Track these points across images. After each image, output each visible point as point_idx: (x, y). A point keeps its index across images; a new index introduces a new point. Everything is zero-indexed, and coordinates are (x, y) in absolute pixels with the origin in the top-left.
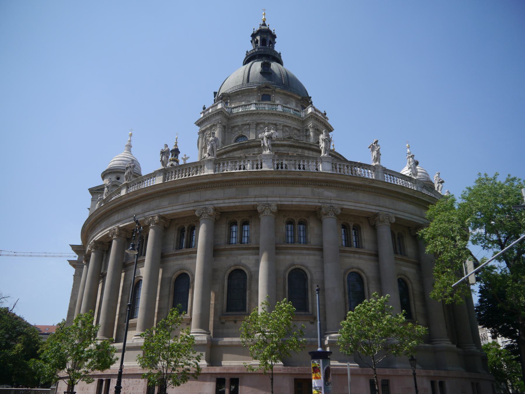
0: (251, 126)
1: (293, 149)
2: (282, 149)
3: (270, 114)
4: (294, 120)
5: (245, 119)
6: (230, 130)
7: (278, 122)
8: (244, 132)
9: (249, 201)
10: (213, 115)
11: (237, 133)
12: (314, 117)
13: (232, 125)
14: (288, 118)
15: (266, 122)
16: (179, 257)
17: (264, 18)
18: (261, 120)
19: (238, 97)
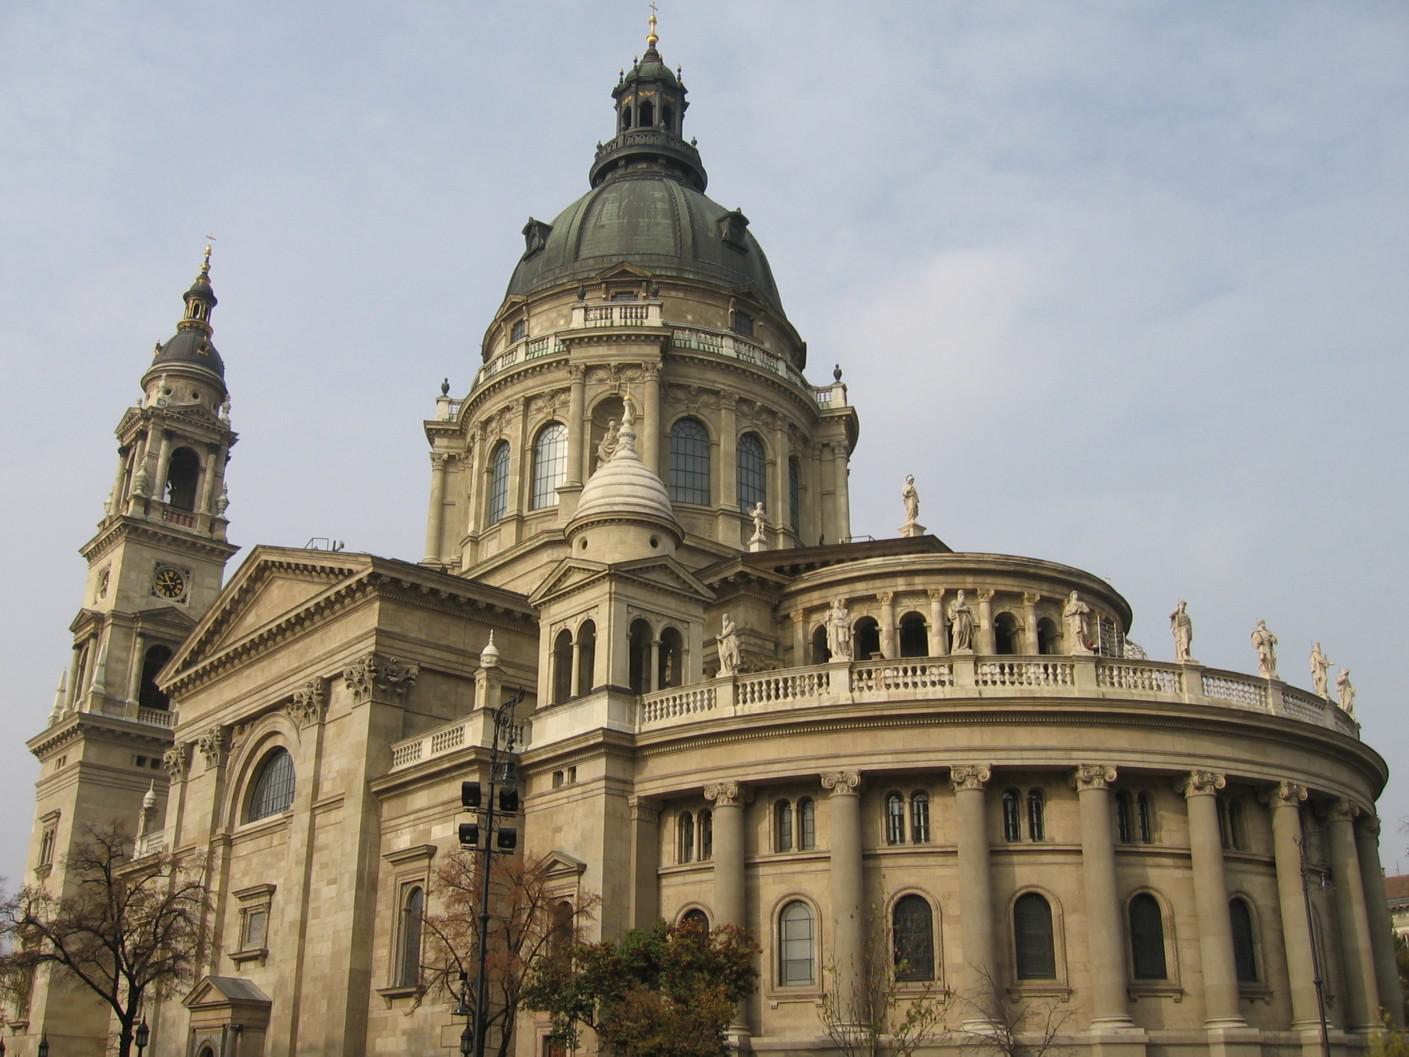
5: (710, 375)
10: (638, 336)
11: (684, 408)
13: (673, 380)
19: (673, 294)
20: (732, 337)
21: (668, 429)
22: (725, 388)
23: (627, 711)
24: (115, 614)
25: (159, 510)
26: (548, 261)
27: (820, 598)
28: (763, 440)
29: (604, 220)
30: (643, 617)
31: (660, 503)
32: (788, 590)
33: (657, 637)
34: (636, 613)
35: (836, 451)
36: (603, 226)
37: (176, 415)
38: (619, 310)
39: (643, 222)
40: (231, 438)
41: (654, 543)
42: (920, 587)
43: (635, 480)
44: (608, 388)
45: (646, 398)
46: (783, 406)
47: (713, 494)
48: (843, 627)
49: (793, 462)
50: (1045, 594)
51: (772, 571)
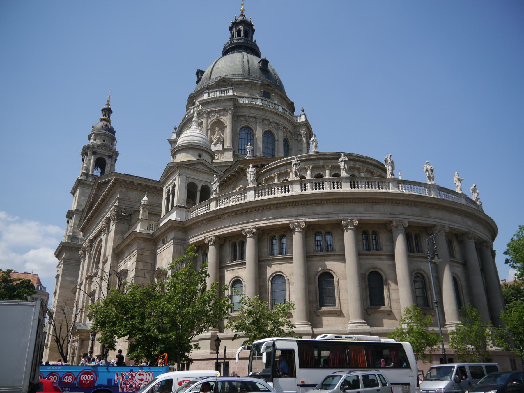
0: (258, 120)
1: (376, 169)
2: (370, 167)
5: (253, 111)
6: (236, 118)
8: (250, 124)
9: (431, 221)
10: (224, 99)
11: (243, 123)
12: (307, 125)
13: (239, 114)
14: (287, 121)
15: (271, 120)
16: (369, 257)
17: (242, 8)
19: (241, 86)
20: (261, 99)
21: (238, 130)
23: (184, 214)
24: (76, 210)
25: (91, 177)
26: (202, 82)
27: (270, 174)
29: (219, 66)
30: (193, 181)
32: (259, 173)
33: (199, 188)
34: (190, 180)
36: (219, 68)
37: (96, 147)
40: (117, 154)
41: (200, 156)
43: (193, 134)
44: (215, 118)
45: (228, 119)
46: (282, 121)
47: (254, 151)
48: (253, 174)
49: (286, 140)
50: (352, 165)
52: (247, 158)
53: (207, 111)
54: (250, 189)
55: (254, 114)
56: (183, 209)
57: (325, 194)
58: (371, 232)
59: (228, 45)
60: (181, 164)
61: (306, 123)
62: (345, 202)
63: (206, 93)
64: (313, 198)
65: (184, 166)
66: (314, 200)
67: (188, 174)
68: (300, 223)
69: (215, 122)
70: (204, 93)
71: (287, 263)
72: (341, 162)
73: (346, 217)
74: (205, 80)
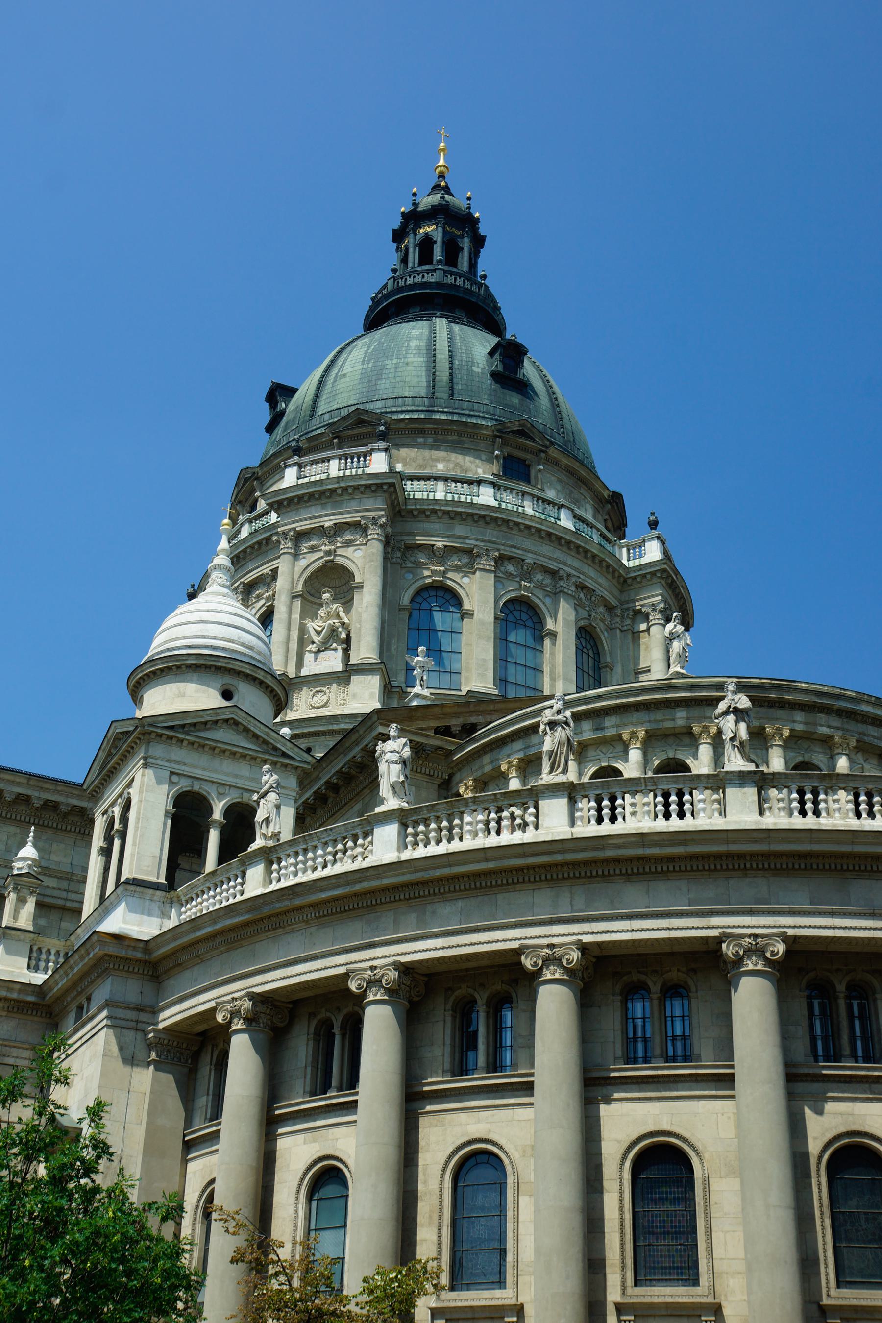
3: (543, 534)
4: (604, 569)
6: (399, 554)
7: (561, 566)
10: (356, 488)
18: (511, 546)
19: (420, 440)
21: (406, 600)
22: (478, 543)
28: (538, 606)
30: (196, 788)
31: (243, 645)
34: (184, 785)
35: (651, 618)
38: (337, 461)
39: (390, 363)
41: (227, 695)
42: (612, 732)
44: (322, 554)
46: (569, 564)
48: (396, 763)
50: (799, 727)
51: (431, 733)
52: (411, 700)
53: (294, 529)
54: (387, 817)
55: (465, 538)
56: (151, 891)
57: (656, 838)
58: (841, 988)
59: (385, 292)
60: (151, 725)
61: (664, 570)
62: (734, 869)
63: (290, 466)
64: (610, 853)
65: (164, 732)
66: (617, 860)
67: (178, 763)
68: (558, 951)
69: (319, 570)
70: (286, 467)
71: (513, 1105)
72: (726, 713)
73: (739, 927)
74: (295, 418)
